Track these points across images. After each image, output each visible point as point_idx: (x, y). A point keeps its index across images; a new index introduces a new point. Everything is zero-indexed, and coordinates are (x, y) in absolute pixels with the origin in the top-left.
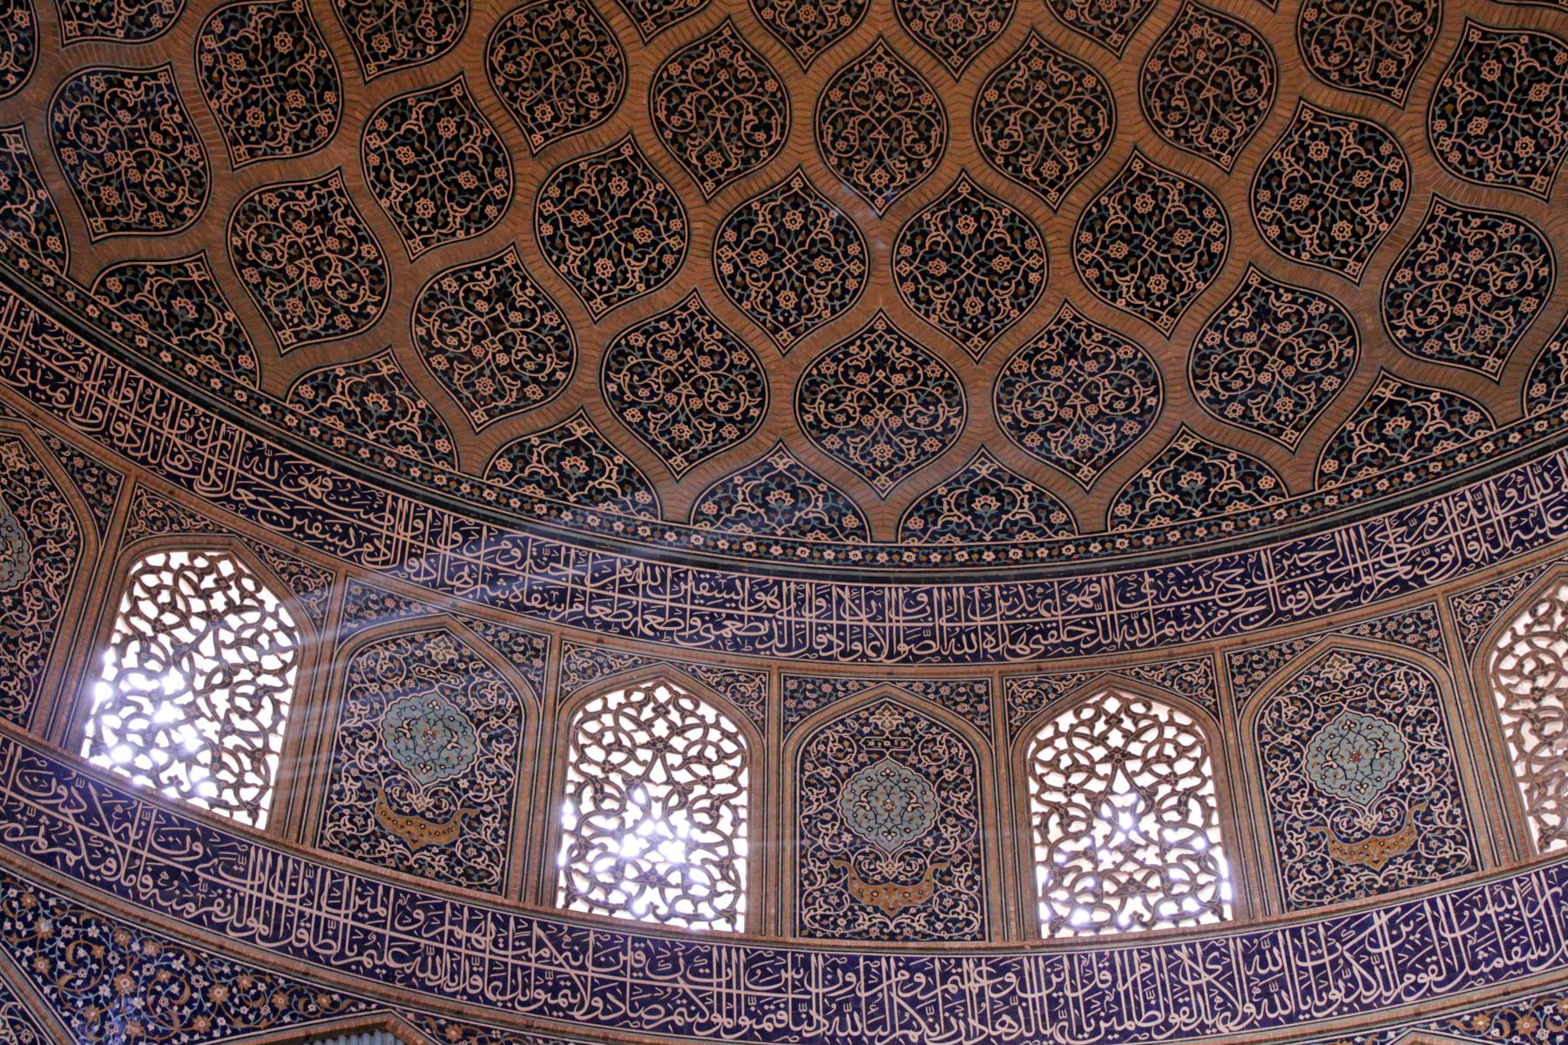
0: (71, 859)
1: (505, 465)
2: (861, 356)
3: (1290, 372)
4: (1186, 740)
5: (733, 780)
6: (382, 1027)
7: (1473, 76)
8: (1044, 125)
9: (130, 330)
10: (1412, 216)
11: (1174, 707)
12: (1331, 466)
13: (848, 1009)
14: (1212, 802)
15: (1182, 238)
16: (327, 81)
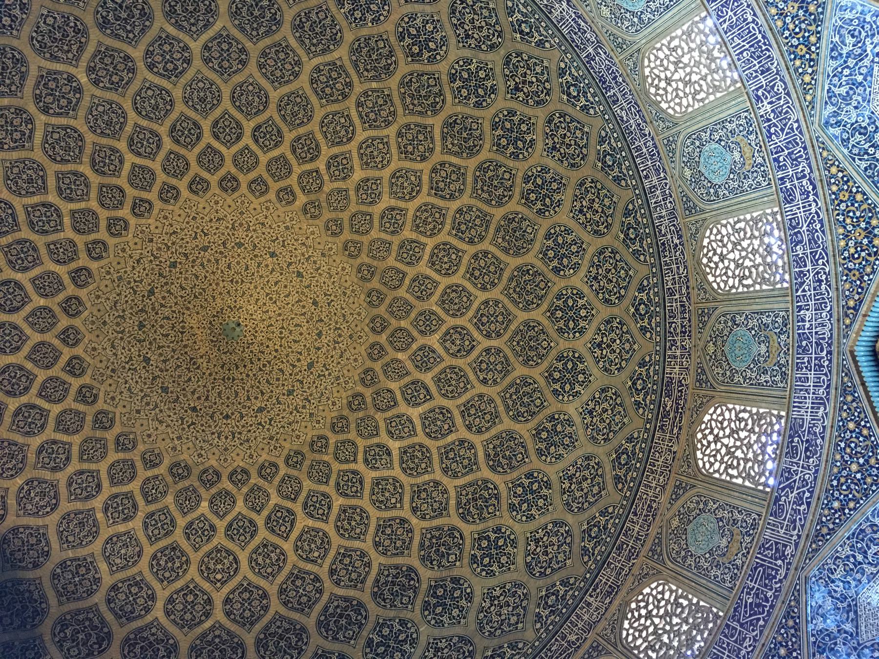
0: (807, 494)
1: (648, 335)
2: (582, 219)
3: (528, 72)
4: (652, 58)
5: (725, 226)
6: (852, 352)
7: (420, 54)
8: (495, 183)
9: (633, 479)
10: (467, 53)
11: (643, 67)
12: (547, 45)
13: (794, 157)
14: (668, 38)
15: (508, 125)
16: (552, 418)
